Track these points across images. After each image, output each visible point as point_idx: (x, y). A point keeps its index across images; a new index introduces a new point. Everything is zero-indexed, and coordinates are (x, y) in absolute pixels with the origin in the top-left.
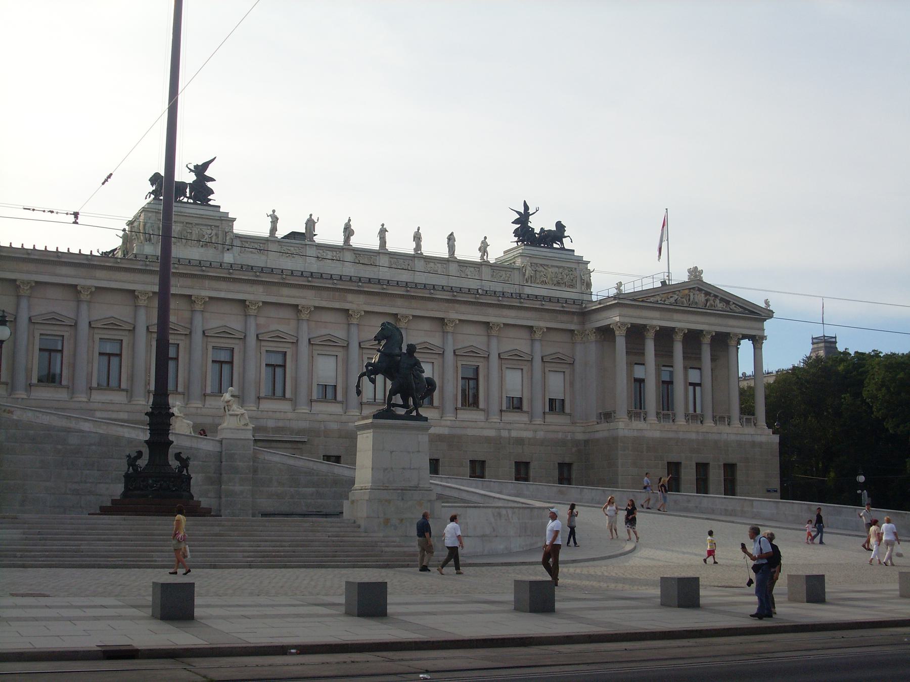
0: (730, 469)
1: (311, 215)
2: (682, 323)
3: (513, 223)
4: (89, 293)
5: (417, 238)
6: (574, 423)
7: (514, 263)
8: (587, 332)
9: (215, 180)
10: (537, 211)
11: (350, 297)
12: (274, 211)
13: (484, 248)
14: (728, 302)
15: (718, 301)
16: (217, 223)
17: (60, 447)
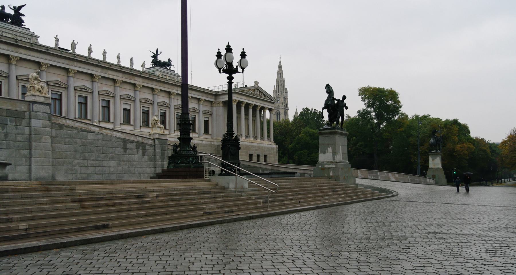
0: (265, 156)
1: (74, 41)
2: (253, 102)
3: (151, 57)
4: (16, 60)
5: (118, 57)
6: (212, 138)
7: (154, 73)
8: (218, 103)
9: (25, 16)
10: (161, 53)
11: (136, 78)
12: (57, 36)
13: (143, 65)
14: (265, 96)
15: (262, 95)
16: (30, 37)
17: (84, 140)
